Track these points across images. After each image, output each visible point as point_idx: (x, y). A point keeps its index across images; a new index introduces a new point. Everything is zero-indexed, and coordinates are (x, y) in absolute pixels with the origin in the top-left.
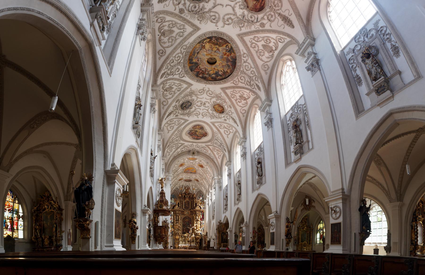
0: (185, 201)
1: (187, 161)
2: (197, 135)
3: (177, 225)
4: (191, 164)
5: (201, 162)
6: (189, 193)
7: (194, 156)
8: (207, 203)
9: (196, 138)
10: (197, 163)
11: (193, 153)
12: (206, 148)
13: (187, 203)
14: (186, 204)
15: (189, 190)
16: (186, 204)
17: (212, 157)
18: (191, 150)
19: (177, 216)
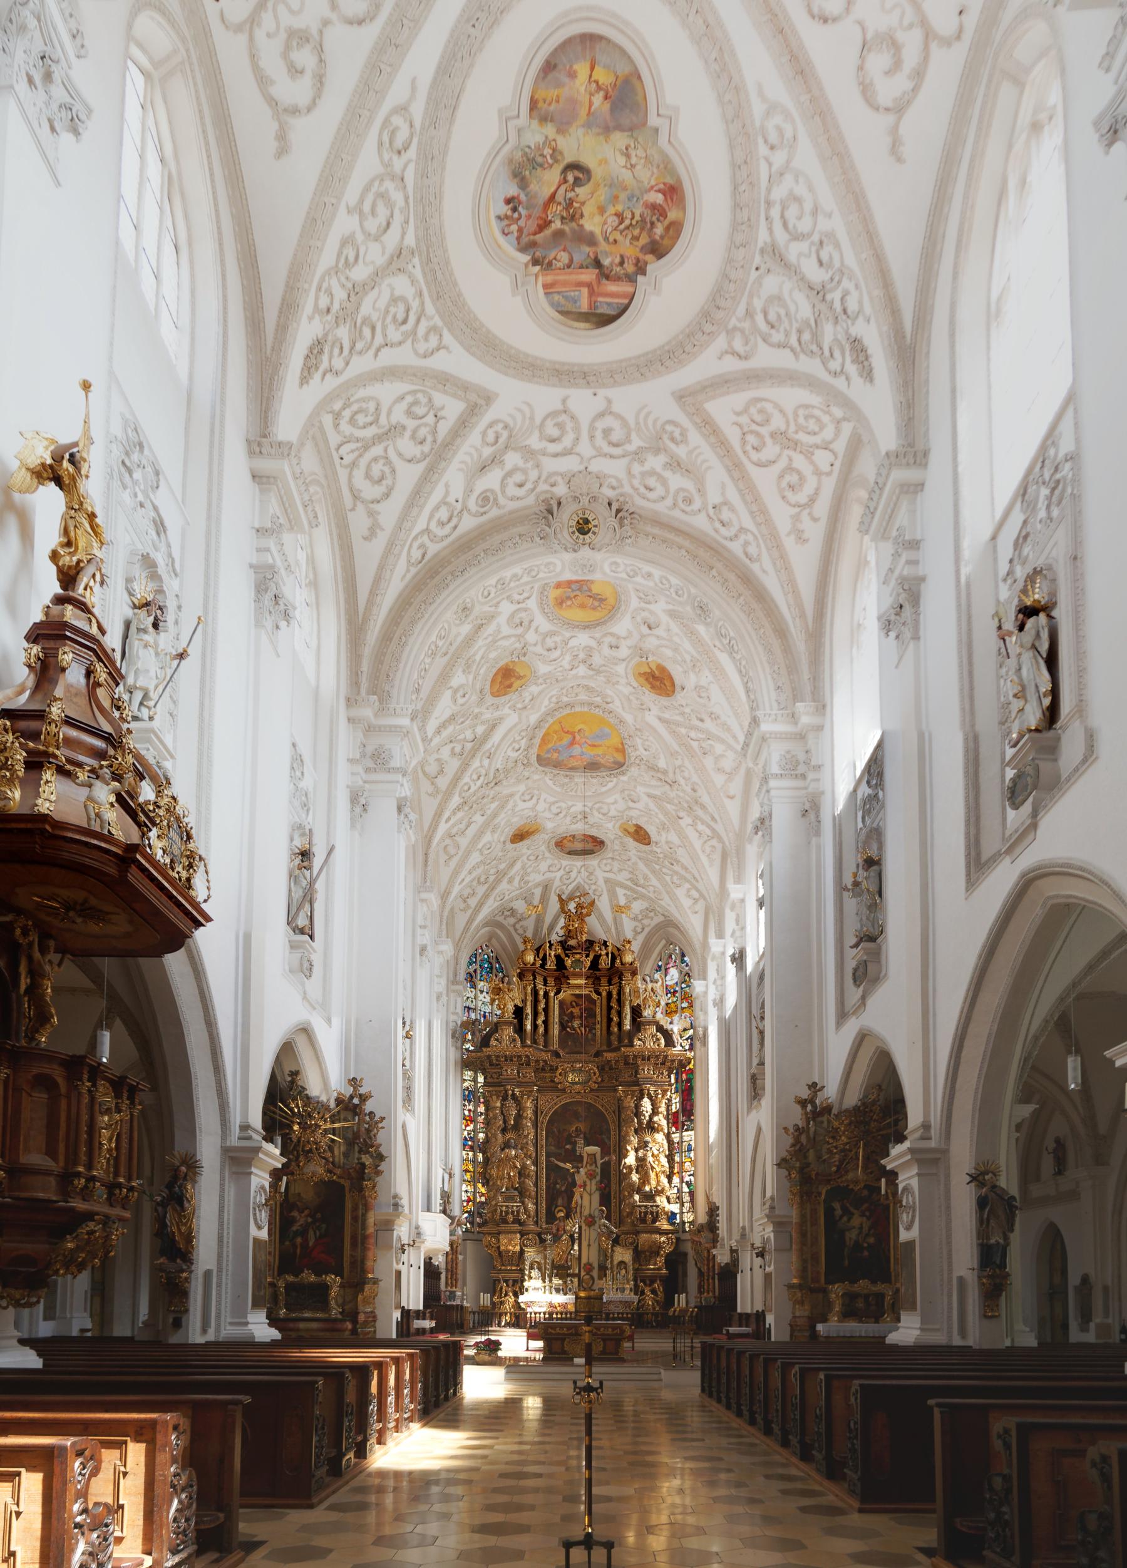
0: (561, 995)
1: (550, 642)
2: (590, 240)
3: (509, 1159)
4: (582, 670)
5: (651, 643)
6: (591, 943)
7: (585, 552)
8: (712, 994)
9: (584, 306)
10: (624, 652)
11: (583, 527)
12: (684, 439)
13: (576, 1011)
14: (572, 1017)
15: (592, 921)
16: (572, 1017)
17: (736, 547)
18: (561, 490)
19: (510, 1102)
